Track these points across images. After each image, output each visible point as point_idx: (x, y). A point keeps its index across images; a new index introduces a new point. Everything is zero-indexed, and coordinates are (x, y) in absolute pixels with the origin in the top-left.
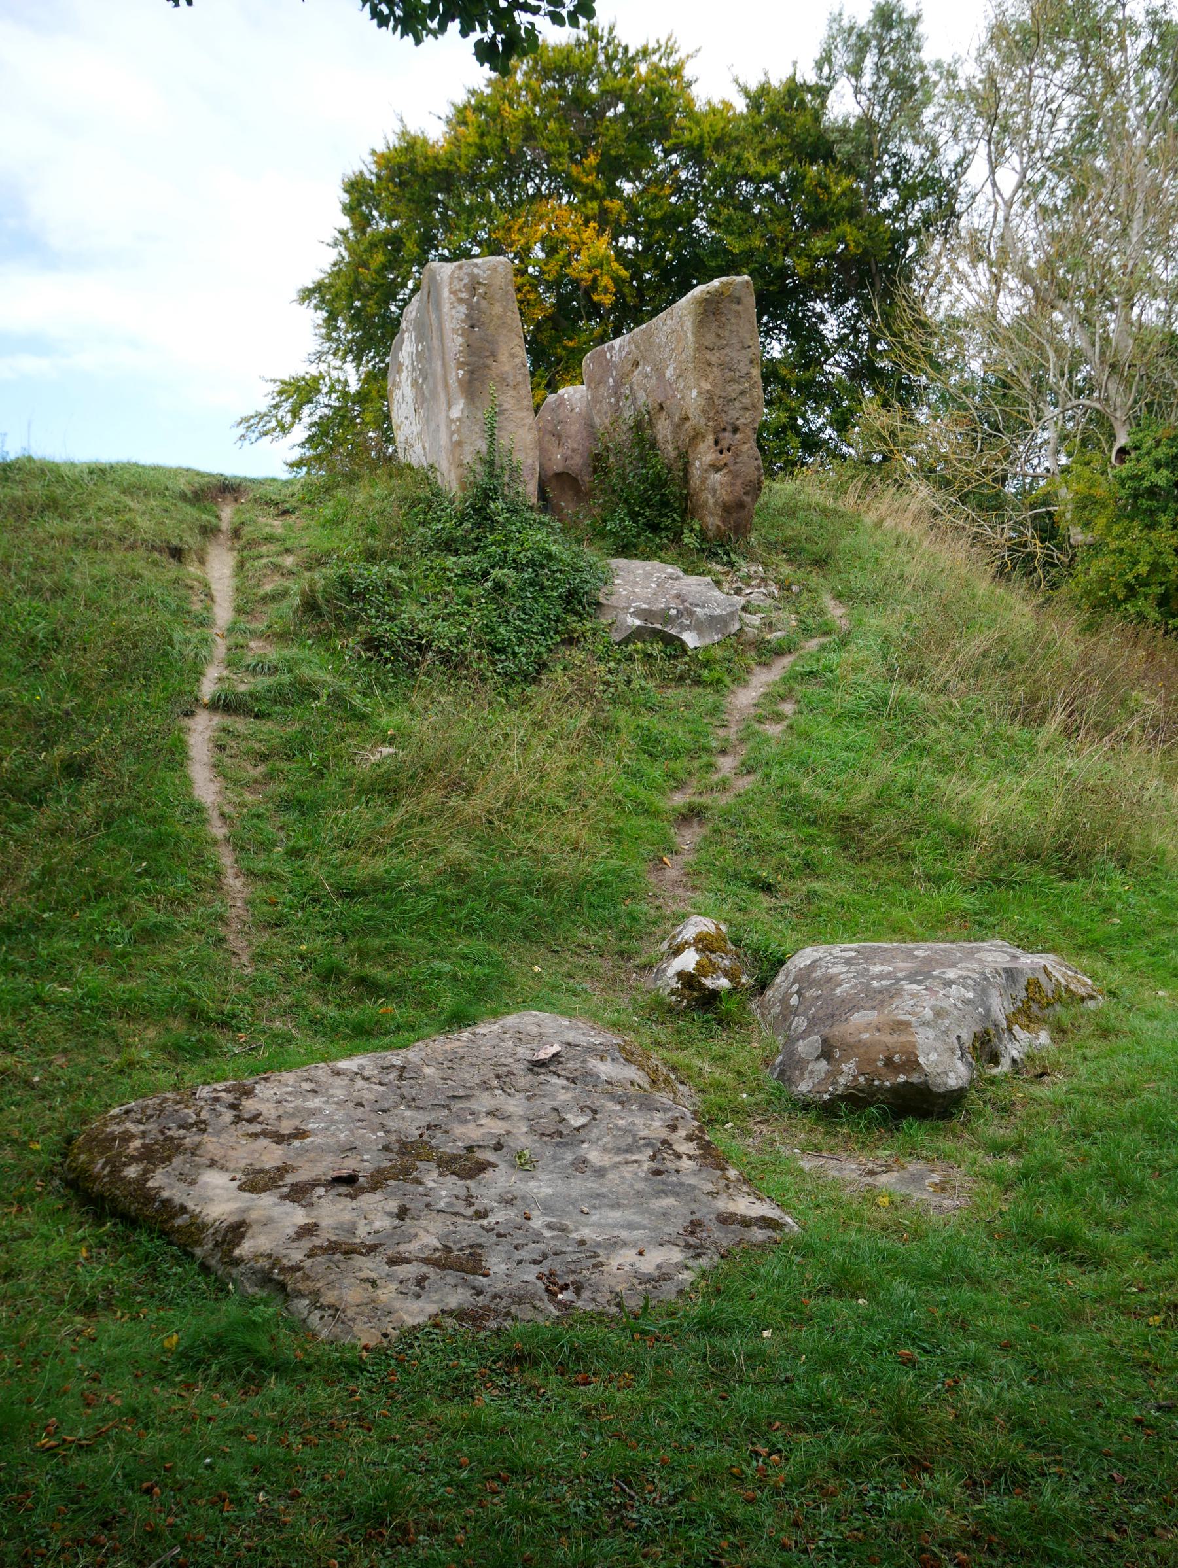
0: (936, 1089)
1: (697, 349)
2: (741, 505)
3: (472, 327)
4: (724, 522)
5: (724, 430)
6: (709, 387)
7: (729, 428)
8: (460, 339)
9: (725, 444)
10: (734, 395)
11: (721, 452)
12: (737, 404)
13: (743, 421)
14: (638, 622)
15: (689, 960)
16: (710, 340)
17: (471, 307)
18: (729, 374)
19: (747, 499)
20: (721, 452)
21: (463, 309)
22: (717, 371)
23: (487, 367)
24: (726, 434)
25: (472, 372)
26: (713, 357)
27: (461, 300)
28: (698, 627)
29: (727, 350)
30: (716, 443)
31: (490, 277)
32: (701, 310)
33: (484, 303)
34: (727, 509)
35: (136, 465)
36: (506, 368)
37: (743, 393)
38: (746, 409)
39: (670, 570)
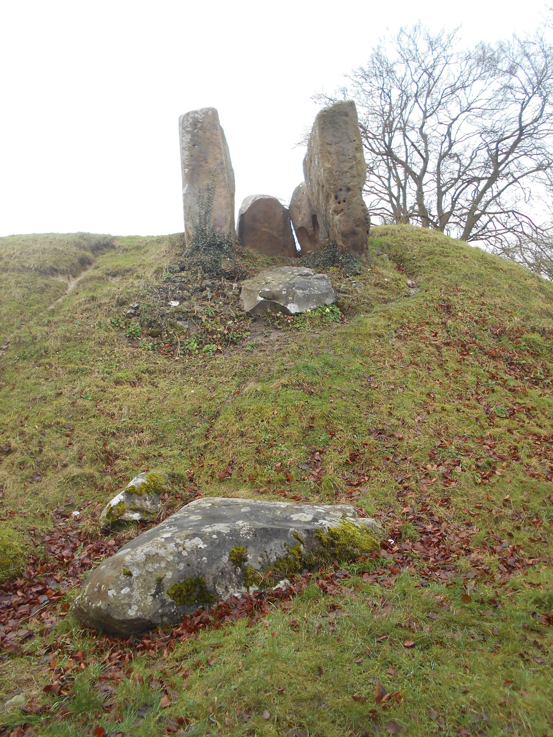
0: (116, 617)
1: (322, 145)
2: (354, 233)
3: (194, 145)
4: (344, 243)
5: (341, 190)
6: (330, 166)
7: (344, 189)
8: (187, 153)
9: (341, 198)
10: (345, 169)
11: (339, 203)
12: (348, 174)
13: (352, 184)
14: (262, 299)
15: (117, 499)
16: (329, 139)
17: (193, 135)
18: (342, 158)
19: (359, 229)
20: (339, 203)
21: (189, 136)
22: (334, 156)
23: (201, 166)
24: (342, 192)
25: (193, 169)
26: (332, 149)
27: (188, 132)
28: (298, 301)
29: (341, 144)
30: (336, 197)
31: (203, 118)
32: (322, 122)
33: (201, 132)
34: (345, 235)
35: (88, 234)
36: (212, 166)
37: (351, 168)
38: (354, 177)
39: (306, 270)
